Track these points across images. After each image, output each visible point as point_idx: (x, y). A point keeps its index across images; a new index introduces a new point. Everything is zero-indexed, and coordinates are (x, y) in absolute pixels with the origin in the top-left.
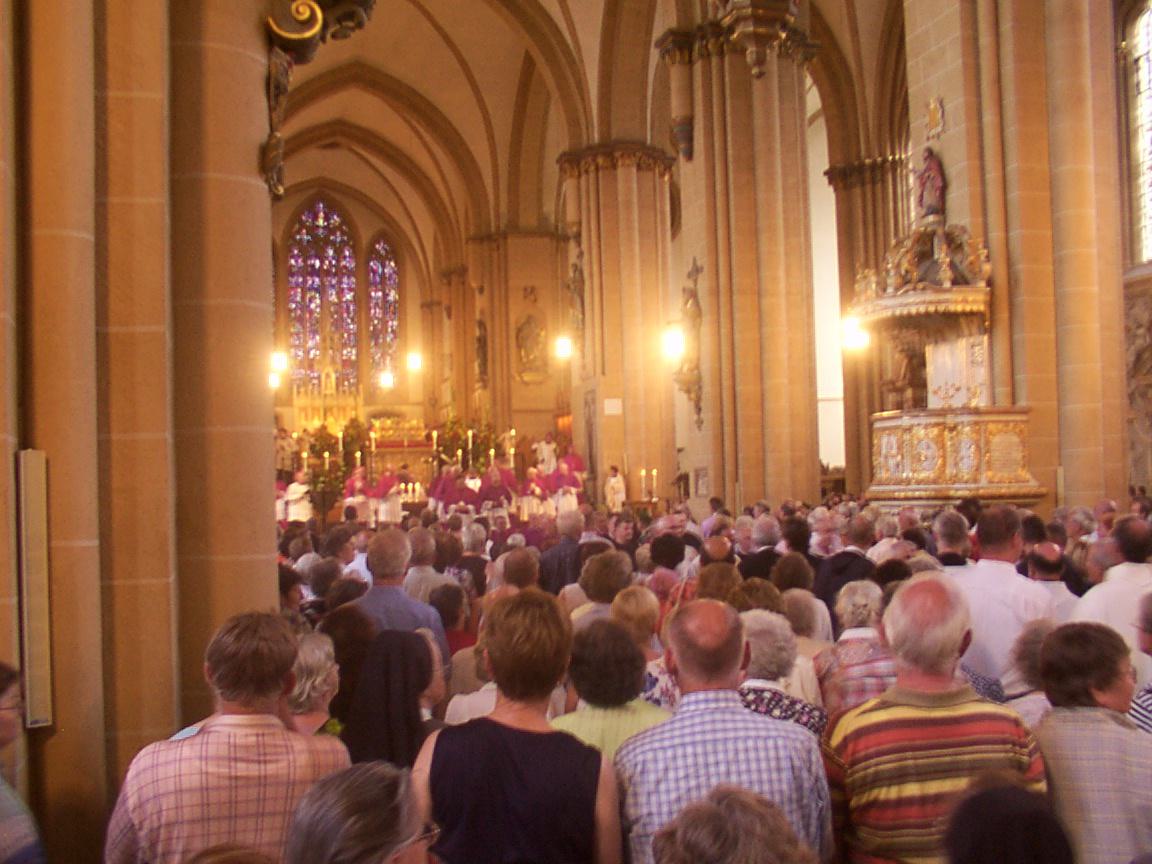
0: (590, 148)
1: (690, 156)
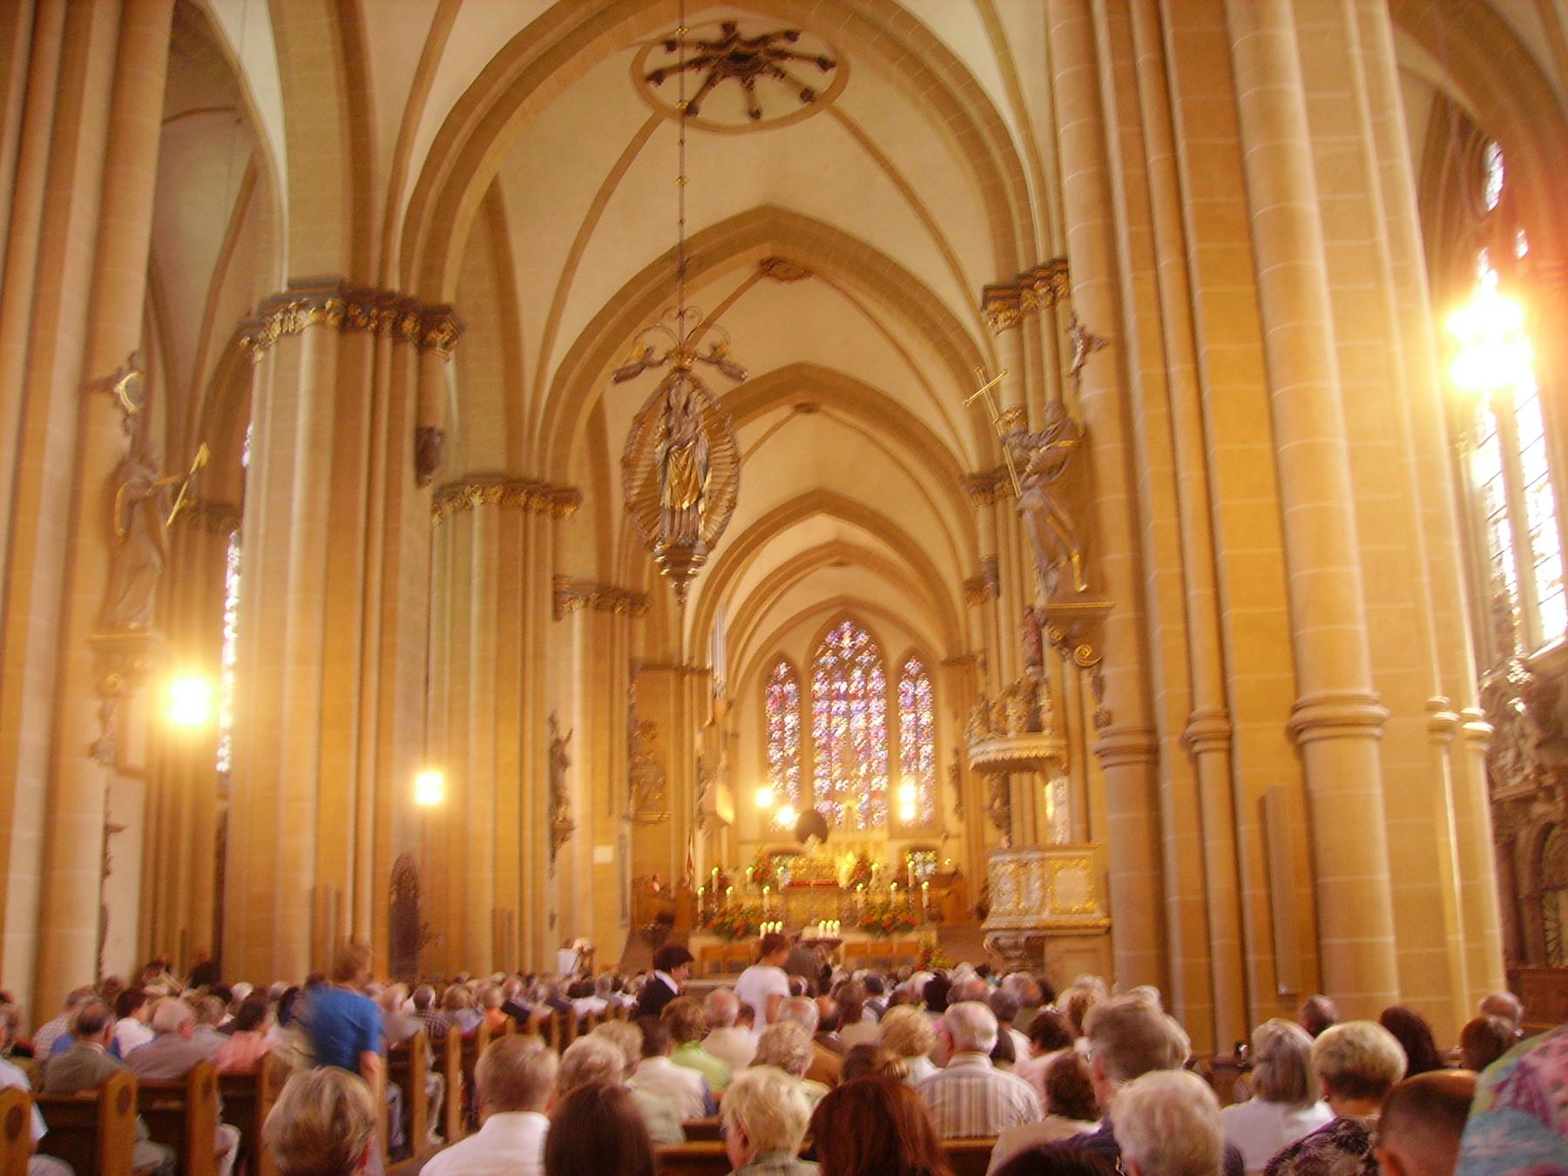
1: (998, 593)
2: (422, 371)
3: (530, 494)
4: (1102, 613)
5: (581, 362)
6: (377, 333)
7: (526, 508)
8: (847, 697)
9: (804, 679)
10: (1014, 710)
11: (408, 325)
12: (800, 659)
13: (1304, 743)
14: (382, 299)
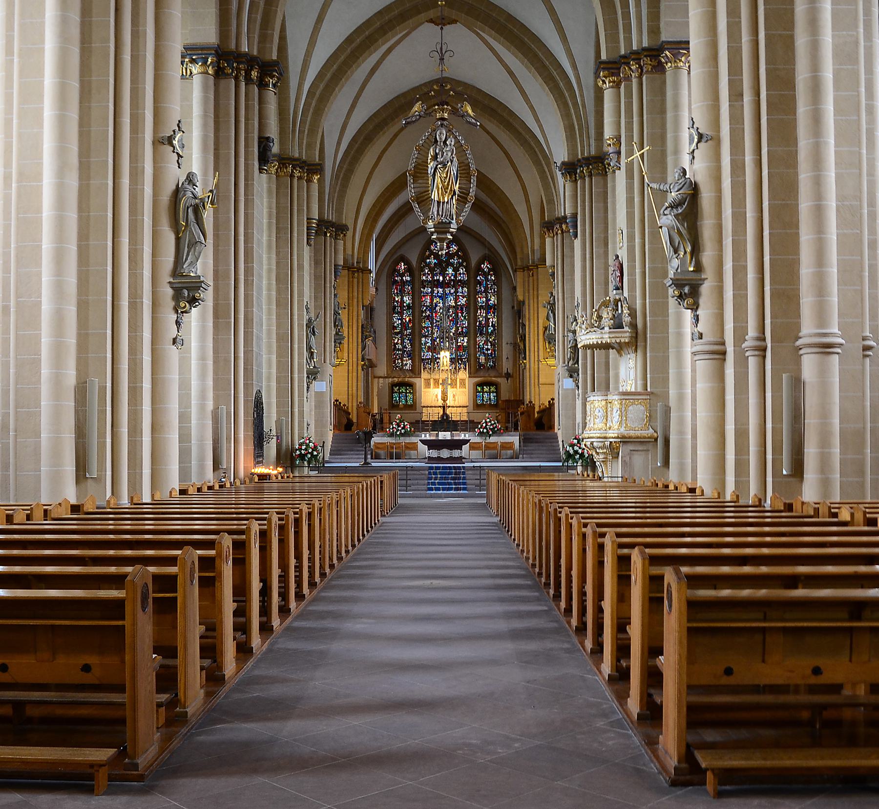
0: (558, 219)
1: (576, 236)
2: (261, 101)
3: (294, 167)
4: (701, 282)
5: (324, 82)
6: (237, 78)
7: (292, 176)
8: (443, 285)
9: (416, 273)
10: (607, 314)
11: (254, 74)
12: (414, 261)
13: (801, 355)
14: (238, 56)
